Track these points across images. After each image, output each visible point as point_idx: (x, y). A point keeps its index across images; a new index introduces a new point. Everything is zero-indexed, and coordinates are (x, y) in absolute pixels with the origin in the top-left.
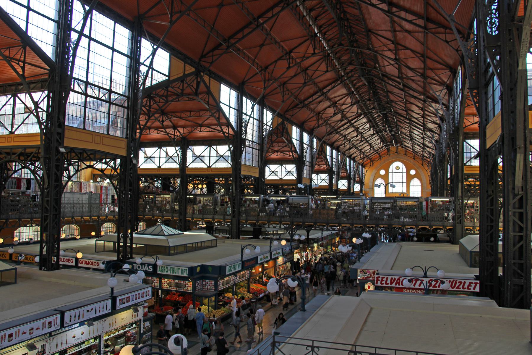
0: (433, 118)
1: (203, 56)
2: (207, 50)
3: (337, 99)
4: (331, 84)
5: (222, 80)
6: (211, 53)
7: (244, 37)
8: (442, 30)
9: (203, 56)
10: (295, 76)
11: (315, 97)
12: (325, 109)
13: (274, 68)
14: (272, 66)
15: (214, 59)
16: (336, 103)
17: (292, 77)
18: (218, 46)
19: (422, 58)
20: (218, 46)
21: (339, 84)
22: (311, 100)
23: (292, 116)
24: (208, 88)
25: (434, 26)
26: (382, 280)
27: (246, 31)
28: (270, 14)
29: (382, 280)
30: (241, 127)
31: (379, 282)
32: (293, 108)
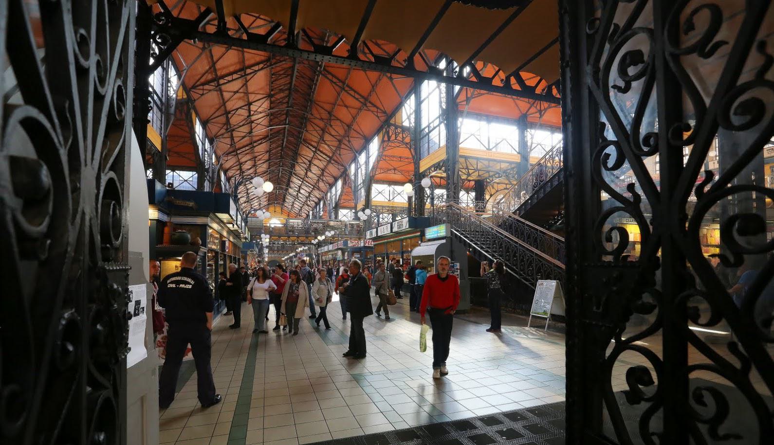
0: (328, 178)
1: (194, 87)
2: (198, 83)
3: (257, 154)
4: (261, 139)
5: (197, 114)
6: (201, 87)
7: (233, 80)
8: (375, 109)
9: (194, 87)
10: (243, 125)
11: (247, 148)
12: (246, 162)
13: (234, 114)
14: (233, 112)
15: (204, 93)
16: (256, 157)
17: (241, 126)
18: (207, 83)
19: (346, 127)
20: (207, 83)
21: (268, 140)
22: (244, 149)
23: (227, 161)
24: (191, 117)
25: (370, 105)
26: (369, 243)
27: (235, 76)
28: (256, 68)
29: (369, 243)
30: (205, 157)
31: (367, 244)
32: (228, 154)
